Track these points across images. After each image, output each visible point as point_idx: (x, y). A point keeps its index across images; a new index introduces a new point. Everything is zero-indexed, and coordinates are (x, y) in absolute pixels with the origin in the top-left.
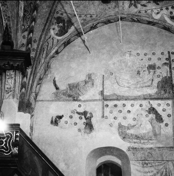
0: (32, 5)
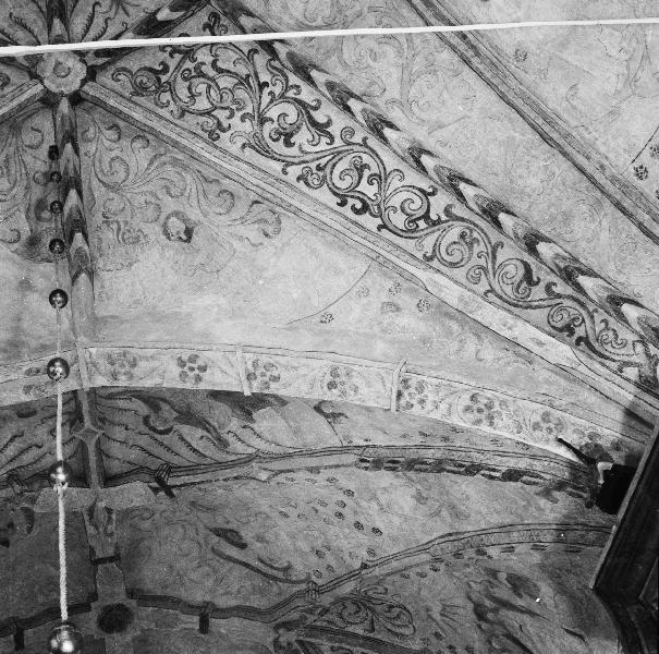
0: (557, 289)
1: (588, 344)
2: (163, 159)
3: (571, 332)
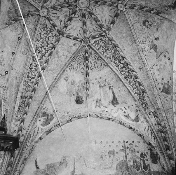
0: (25, 103)
1: (19, 110)
2: (32, 31)
3: (20, 107)
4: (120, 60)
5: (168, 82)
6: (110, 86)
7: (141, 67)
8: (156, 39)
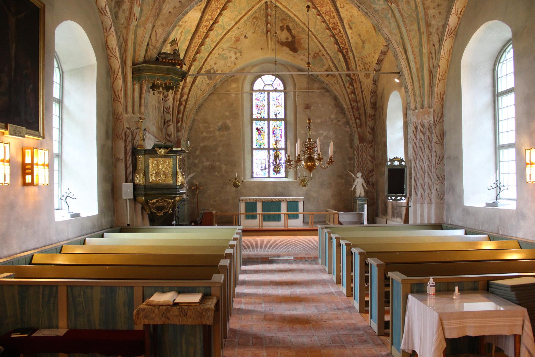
4: (212, 19)
5: (217, 70)
6: (184, 31)
7: (214, 40)
8: (245, 36)
